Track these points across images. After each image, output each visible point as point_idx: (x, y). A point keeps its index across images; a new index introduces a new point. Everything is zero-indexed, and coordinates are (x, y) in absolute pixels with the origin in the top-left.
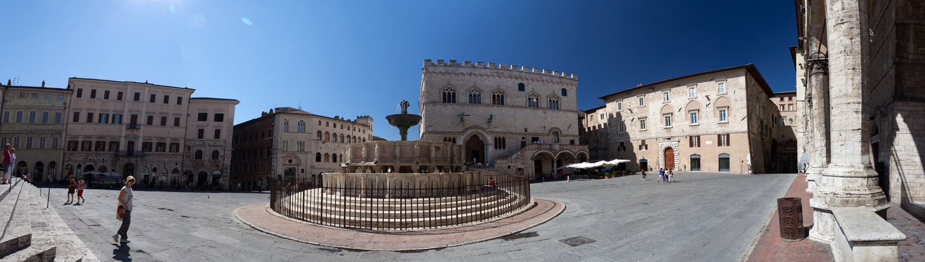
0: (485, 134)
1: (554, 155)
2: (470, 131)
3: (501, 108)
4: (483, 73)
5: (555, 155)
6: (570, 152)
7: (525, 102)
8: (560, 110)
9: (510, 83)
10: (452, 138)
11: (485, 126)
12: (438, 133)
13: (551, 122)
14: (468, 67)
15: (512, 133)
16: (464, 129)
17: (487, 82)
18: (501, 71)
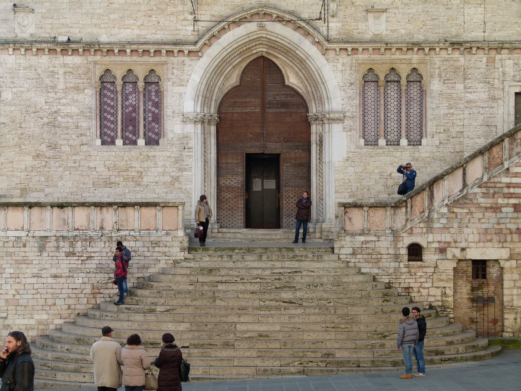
10: (141, 73)
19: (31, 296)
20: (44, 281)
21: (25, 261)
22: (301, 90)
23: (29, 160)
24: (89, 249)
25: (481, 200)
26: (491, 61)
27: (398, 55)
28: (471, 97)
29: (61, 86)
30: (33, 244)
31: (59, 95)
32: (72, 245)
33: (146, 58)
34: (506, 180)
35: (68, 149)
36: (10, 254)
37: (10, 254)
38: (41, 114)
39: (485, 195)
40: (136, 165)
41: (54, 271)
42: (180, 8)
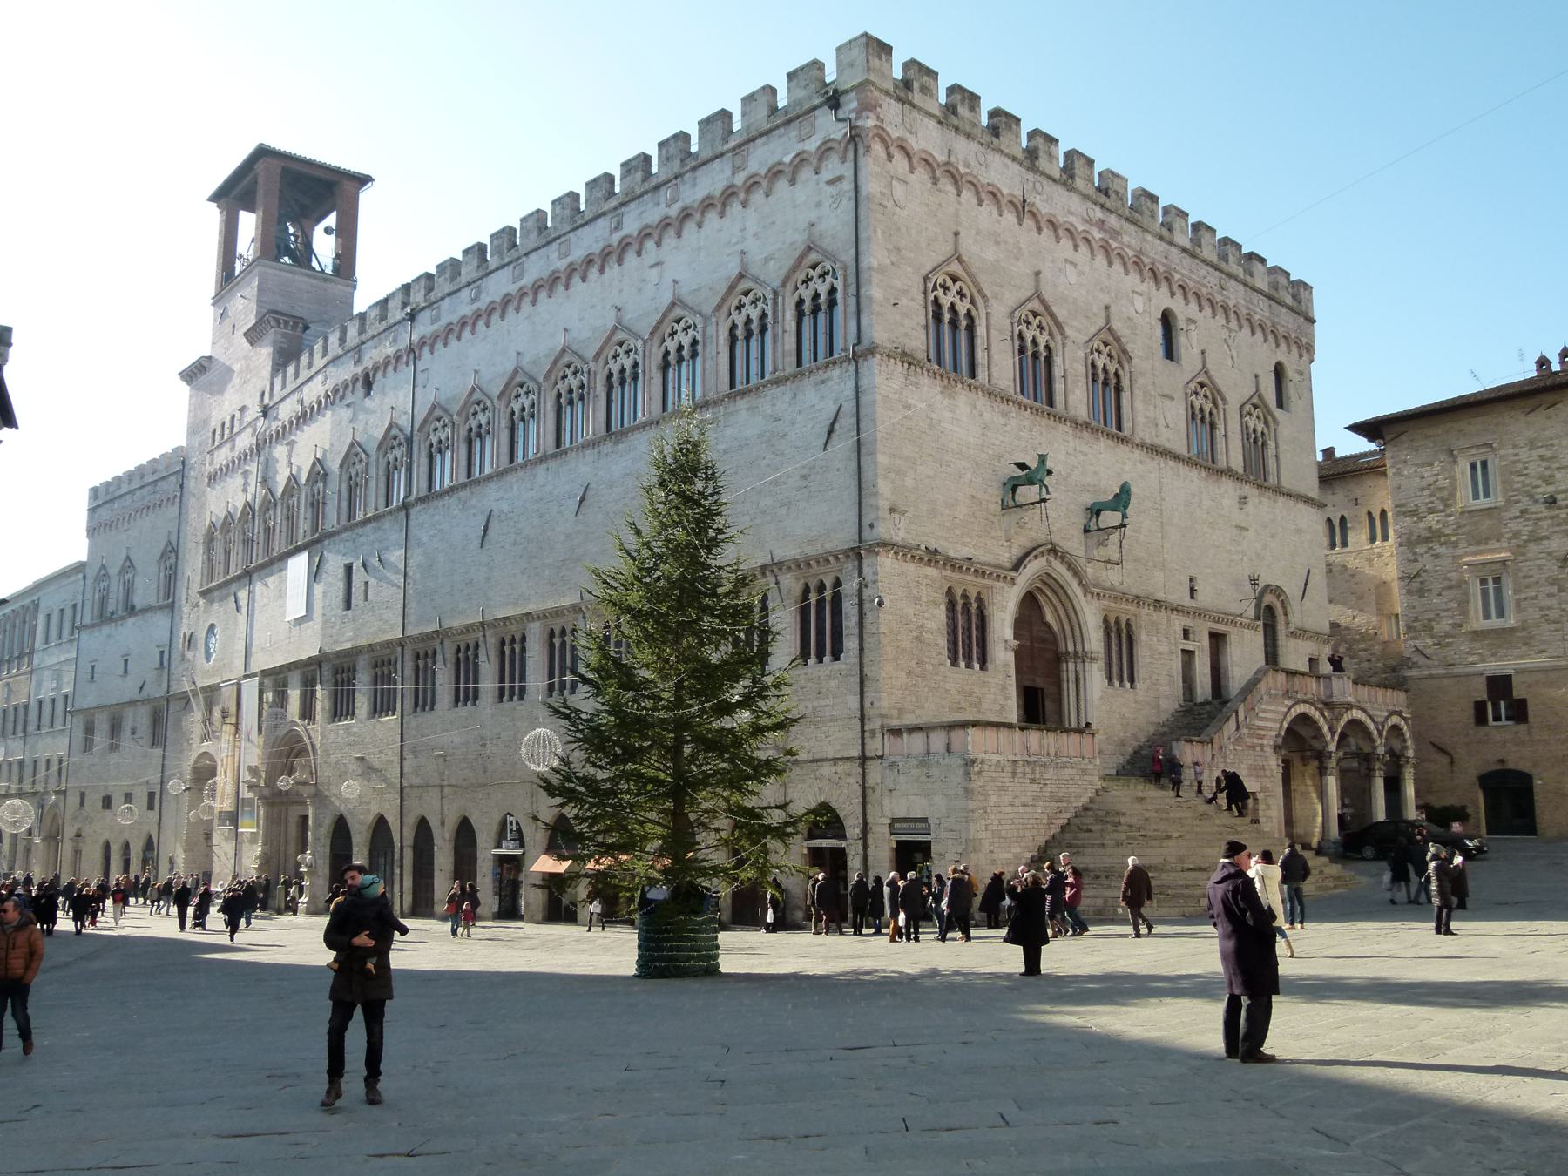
0: (1079, 591)
1: (1330, 728)
2: (1034, 567)
3: (1123, 450)
4: (1061, 218)
5: (1333, 736)
6: (1368, 722)
7: (1183, 425)
8: (1278, 491)
9: (1139, 303)
10: (973, 595)
11: (1073, 543)
12: (932, 557)
13: (1258, 555)
14: (1014, 159)
15: (1158, 604)
16: (1017, 552)
17: (1072, 275)
18: (1112, 221)
19: (1008, 827)
20: (1016, 809)
21: (1002, 789)
22: (1055, 628)
23: (902, 678)
24: (1045, 776)
25: (1247, 740)
26: (1169, 620)
27: (1123, 606)
28: (1161, 649)
29: (924, 599)
30: (1008, 769)
31: (924, 608)
32: (1033, 772)
33: (979, 580)
34: (1258, 723)
35: (929, 667)
36: (993, 780)
37: (993, 780)
38: (912, 626)
39: (1250, 735)
40: (976, 690)
41: (1023, 799)
42: (999, 533)
